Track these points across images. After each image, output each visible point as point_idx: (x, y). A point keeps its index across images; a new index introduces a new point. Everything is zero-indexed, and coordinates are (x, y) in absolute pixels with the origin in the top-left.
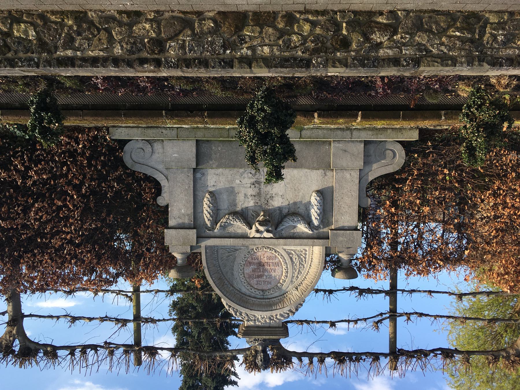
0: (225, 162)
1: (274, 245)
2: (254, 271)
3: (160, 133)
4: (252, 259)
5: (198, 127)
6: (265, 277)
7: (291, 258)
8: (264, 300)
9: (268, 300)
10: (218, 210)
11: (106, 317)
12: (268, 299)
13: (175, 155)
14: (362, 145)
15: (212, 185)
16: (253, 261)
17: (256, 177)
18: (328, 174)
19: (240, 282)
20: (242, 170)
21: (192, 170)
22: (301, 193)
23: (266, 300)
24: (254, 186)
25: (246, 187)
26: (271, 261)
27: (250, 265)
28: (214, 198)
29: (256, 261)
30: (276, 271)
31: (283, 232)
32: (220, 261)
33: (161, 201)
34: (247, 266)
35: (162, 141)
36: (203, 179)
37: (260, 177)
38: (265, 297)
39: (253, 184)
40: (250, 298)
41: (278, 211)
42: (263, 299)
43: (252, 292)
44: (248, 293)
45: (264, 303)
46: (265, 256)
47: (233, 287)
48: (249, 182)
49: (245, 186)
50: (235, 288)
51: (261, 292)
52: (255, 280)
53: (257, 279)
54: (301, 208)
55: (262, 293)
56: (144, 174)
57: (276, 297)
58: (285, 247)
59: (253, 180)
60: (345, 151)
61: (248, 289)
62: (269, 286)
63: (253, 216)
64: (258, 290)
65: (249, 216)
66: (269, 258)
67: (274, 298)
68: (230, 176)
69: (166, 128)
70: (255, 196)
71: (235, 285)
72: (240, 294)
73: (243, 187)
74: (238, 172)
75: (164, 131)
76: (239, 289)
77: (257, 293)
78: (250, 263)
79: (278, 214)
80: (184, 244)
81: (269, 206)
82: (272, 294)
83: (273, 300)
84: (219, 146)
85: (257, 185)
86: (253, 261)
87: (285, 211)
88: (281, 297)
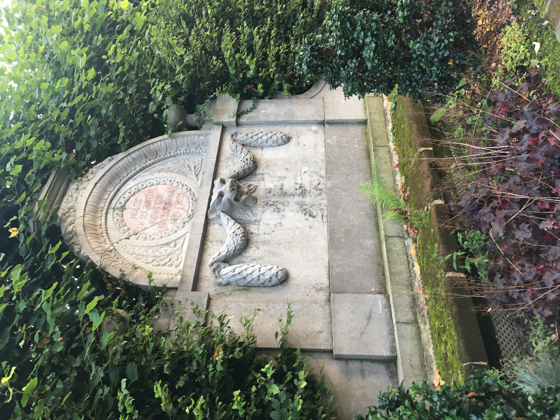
0: (335, 153)
6: (145, 210)
7: (167, 244)
10: (262, 148)
12: (107, 212)
14: (385, 353)
15: (300, 141)
16: (176, 195)
17: (314, 191)
18: (321, 293)
19: (145, 179)
20: (323, 173)
22: (283, 251)
28: (280, 141)
29: (174, 199)
31: (216, 226)
32: (184, 157)
39: (301, 187)
41: (253, 219)
45: (102, 205)
46: (181, 211)
47: (141, 170)
50: (138, 172)
52: (144, 198)
54: (257, 251)
55: (118, 205)
58: (188, 235)
59: (307, 187)
60: (369, 318)
61: (130, 189)
64: (125, 203)
67: (106, 220)
68: (313, 160)
70: (281, 189)
72: (126, 178)
73: (296, 176)
76: (134, 177)
78: (173, 192)
81: (263, 207)
83: (103, 218)
84: (360, 146)
85: (299, 192)
86: (176, 195)
87: (253, 228)
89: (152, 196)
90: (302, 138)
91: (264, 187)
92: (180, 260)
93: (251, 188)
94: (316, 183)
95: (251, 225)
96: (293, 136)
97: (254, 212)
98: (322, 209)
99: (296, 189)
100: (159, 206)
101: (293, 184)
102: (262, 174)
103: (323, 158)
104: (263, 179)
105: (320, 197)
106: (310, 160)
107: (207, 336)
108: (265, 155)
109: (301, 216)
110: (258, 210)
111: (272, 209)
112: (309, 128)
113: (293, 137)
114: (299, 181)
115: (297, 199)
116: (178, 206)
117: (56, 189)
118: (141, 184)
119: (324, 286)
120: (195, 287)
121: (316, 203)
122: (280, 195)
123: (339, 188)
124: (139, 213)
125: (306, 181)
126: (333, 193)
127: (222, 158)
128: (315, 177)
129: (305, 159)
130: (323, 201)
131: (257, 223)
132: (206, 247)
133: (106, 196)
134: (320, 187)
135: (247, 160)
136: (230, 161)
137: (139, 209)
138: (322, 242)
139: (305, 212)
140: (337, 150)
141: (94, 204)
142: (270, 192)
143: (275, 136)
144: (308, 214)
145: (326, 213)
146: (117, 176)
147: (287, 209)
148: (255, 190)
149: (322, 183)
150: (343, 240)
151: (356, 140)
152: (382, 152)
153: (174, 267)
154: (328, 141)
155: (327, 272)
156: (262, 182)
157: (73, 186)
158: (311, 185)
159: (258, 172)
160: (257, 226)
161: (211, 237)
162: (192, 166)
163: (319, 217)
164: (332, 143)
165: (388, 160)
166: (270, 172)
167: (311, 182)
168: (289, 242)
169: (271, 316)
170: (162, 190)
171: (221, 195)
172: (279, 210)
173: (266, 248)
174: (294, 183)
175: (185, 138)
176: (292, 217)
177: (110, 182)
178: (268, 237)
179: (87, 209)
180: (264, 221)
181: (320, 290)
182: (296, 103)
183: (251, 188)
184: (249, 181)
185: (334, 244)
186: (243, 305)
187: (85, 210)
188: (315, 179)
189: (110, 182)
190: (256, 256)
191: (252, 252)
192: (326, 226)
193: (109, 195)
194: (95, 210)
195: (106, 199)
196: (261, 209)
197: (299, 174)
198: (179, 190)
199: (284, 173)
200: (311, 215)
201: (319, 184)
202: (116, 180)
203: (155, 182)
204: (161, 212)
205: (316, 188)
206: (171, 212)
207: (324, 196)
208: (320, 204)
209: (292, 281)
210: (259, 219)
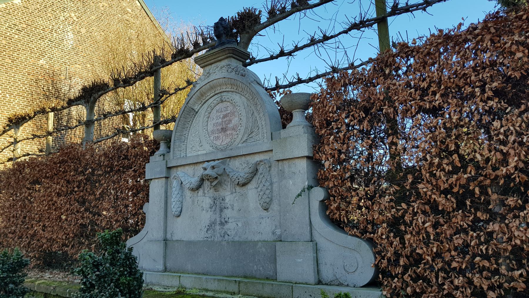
1: (213, 152)
2: (230, 121)
4: (232, 134)
9: (216, 92)
11: (424, 9)
13: (299, 260)
18: (170, 236)
20: (237, 239)
29: (228, 132)
33: (319, 194)
35: (320, 282)
36: (274, 228)
38: (219, 95)
39: (226, 222)
41: (206, 192)
45: (219, 88)
46: (221, 140)
48: (230, 224)
49: (233, 220)
56: (346, 233)
59: (226, 226)
62: (218, 107)
66: (218, 138)
70: (225, 208)
71: (245, 100)
78: (233, 129)
79: (206, 188)
80: (285, 139)
85: (223, 220)
87: (201, 191)
88: (206, 99)
94: (229, 233)
96: (269, 213)
103: (249, 239)
104: (232, 193)
105: (219, 236)
109: (208, 223)
111: (212, 203)
112: (278, 227)
114: (230, 220)
115: (218, 220)
125: (231, 226)
128: (233, 233)
132: (191, 166)
134: (226, 236)
138: (193, 237)
140: (251, 251)
145: (210, 240)
151: (261, 268)
154: (260, 244)
164: (258, 247)
165: (227, 289)
170: (235, 120)
171: (205, 169)
172: (211, 208)
176: (206, 217)
180: (205, 198)
194: (212, 88)
199: (236, 208)
204: (220, 128)
205: (225, 233)
207: (220, 239)
208: (214, 236)
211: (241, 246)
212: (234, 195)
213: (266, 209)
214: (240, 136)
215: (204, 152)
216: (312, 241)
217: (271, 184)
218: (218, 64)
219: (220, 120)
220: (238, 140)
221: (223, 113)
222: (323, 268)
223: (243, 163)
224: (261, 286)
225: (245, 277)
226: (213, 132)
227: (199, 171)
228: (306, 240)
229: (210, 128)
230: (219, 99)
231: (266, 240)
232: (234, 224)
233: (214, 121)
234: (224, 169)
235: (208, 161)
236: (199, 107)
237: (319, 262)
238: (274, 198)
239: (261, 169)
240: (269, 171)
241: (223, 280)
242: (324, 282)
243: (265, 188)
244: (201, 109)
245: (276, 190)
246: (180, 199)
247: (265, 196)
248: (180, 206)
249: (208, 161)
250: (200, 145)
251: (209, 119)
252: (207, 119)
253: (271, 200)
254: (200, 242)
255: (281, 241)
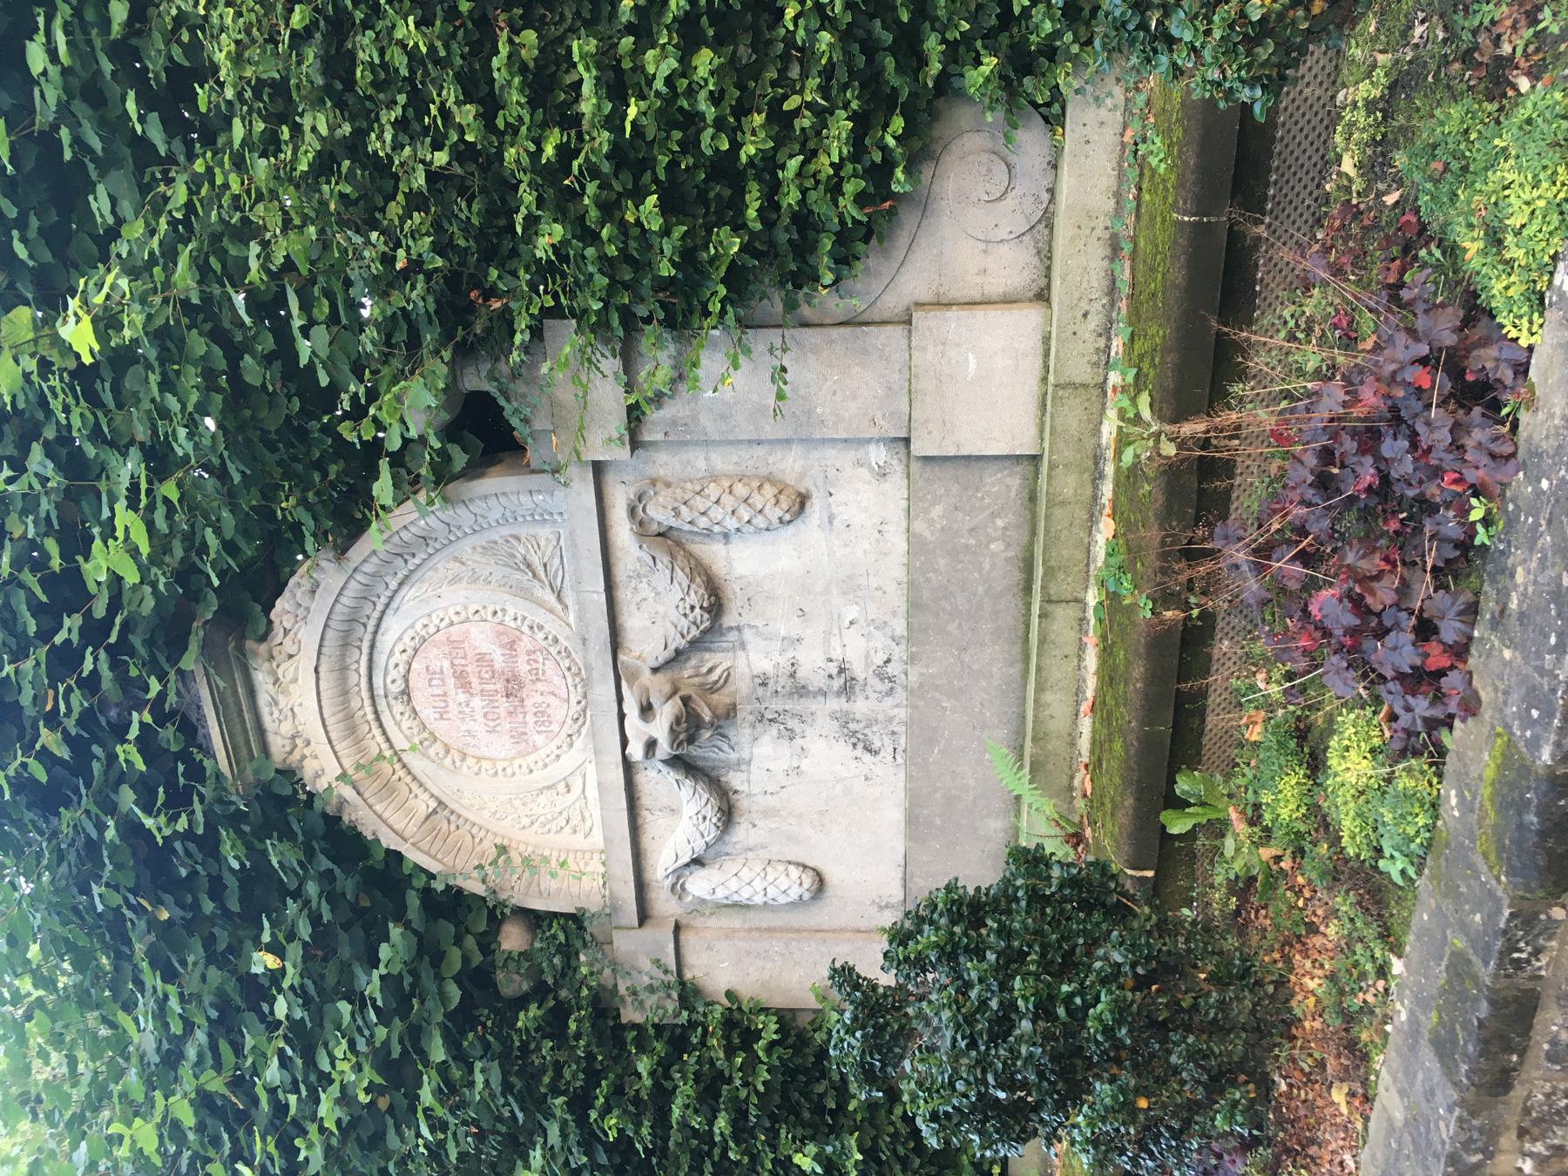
0: (935, 571)
1: (593, 735)
2: (481, 658)
3: (1085, 306)
4: (529, 653)
5: (1098, 477)
6: (462, 697)
8: (367, 702)
9: (370, 717)
10: (726, 536)
12: (376, 712)
13: (972, 365)
20: (900, 627)
21: (904, 435)
23: (368, 709)
24: (835, 672)
25: (826, 641)
26: (530, 719)
27: (503, 646)
29: (523, 668)
30: (493, 737)
32: (505, 531)
34: (499, 634)
35: (1042, 296)
36: (863, 472)
37: (873, 696)
38: (382, 705)
39: (841, 671)
40: (365, 650)
41: (733, 756)
42: (372, 697)
43: (392, 653)
44: (386, 641)
46: (551, 699)
47: (401, 584)
49: (835, 641)
51: (400, 685)
52: (446, 664)
53: (448, 671)
55: (395, 689)
57: (388, 740)
59: (858, 669)
61: (400, 639)
62: (427, 713)
63: (711, 670)
64: (407, 681)
65: (707, 656)
67: (384, 733)
68: (874, 582)
69: (1106, 332)
70: (793, 675)
72: (376, 615)
74: (894, 614)
75: (1095, 322)
76: (394, 605)
77: (393, 674)
78: (512, 645)
81: (754, 727)
82: (398, 724)
83: (376, 731)
84: (1009, 545)
85: (837, 683)
87: (735, 780)
89: (465, 657)
90: (839, 496)
91: (747, 670)
92: (588, 824)
93: (714, 676)
94: (879, 659)
95: (731, 773)
97: (734, 740)
98: (893, 733)
99: (830, 676)
100: (491, 687)
101: (821, 662)
102: (738, 629)
103: (900, 573)
104: (743, 646)
105: (889, 701)
106: (863, 581)
107: (688, 994)
108: (739, 562)
109: (843, 749)
110: (741, 733)
111: (774, 730)
112: (861, 454)
113: (815, 494)
114: (837, 654)
115: (835, 704)
116: (540, 686)
117: (230, 700)
118: (418, 626)
119: (893, 901)
120: (644, 917)
121: (881, 717)
122: (791, 694)
123: (937, 688)
124: (453, 707)
125: (858, 651)
126: (921, 703)
127: (620, 574)
129: (850, 577)
130: (896, 711)
131: (743, 767)
132: (640, 821)
133: (353, 678)
134: (891, 669)
135: (692, 608)
136: (644, 585)
137: (445, 694)
138: (893, 814)
139: (854, 740)
141: (340, 715)
142: (764, 684)
143: (760, 517)
144: (860, 746)
145: (903, 741)
146: (353, 620)
147: (809, 731)
148: (726, 681)
149: (894, 658)
150: (938, 821)
151: (1000, 523)
152: (1064, 616)
153: (580, 836)
154: (919, 526)
155: (900, 875)
156: (741, 654)
157: (261, 678)
158: (867, 665)
159: (729, 620)
160: (744, 776)
161: (645, 800)
162: (535, 560)
163: (887, 754)
164: (927, 534)
165: (1071, 649)
166: (759, 623)
167: (867, 657)
168: (822, 813)
169: (796, 964)
170: (481, 638)
171: (651, 745)
173: (773, 826)
174: (823, 657)
175: (492, 501)
176: (825, 752)
177: (346, 644)
178: (772, 801)
179: (333, 735)
180: (759, 761)
181: (887, 906)
182: (816, 351)
183: (714, 676)
184: (709, 650)
185: (913, 822)
186: (742, 944)
187: (330, 742)
188: (879, 645)
189: (346, 644)
190: (752, 842)
191: (742, 833)
192: (902, 775)
193: (357, 670)
194: (352, 730)
195: (358, 685)
196: (748, 731)
197: (836, 631)
198: (525, 639)
200: (868, 749)
201: (888, 661)
202: (352, 634)
203: (455, 619)
204: (504, 705)
205: (882, 676)
206: (527, 703)
208: (890, 720)
209: (830, 891)
210: (746, 755)
211: (923, 607)
212: (748, 634)
213: (802, 502)
214: (540, 617)
215: (591, 770)
216: (909, 322)
217: (714, 478)
218: (263, 700)
219: (477, 702)
220: (553, 627)
221: (452, 692)
222: (996, 285)
223: (638, 598)
224: (1058, 512)
225: (1028, 589)
226: (519, 736)
227: (659, 782)
228: (905, 341)
229: (499, 746)
230: (398, 707)
231: (904, 504)
232: (851, 636)
233: (479, 727)
234: (655, 670)
235: (624, 742)
236: (419, 791)
237: (978, 298)
238: (763, 471)
239: (659, 513)
240: (668, 485)
241: (1039, 669)
242: (1043, 282)
243: (728, 500)
244: (429, 785)
245: (735, 459)
246: (758, 869)
247: (758, 501)
248: (781, 868)
249: (624, 742)
250: (561, 787)
251: (468, 750)
252: (470, 761)
253: (769, 479)
254: (909, 778)
255: (907, 441)
